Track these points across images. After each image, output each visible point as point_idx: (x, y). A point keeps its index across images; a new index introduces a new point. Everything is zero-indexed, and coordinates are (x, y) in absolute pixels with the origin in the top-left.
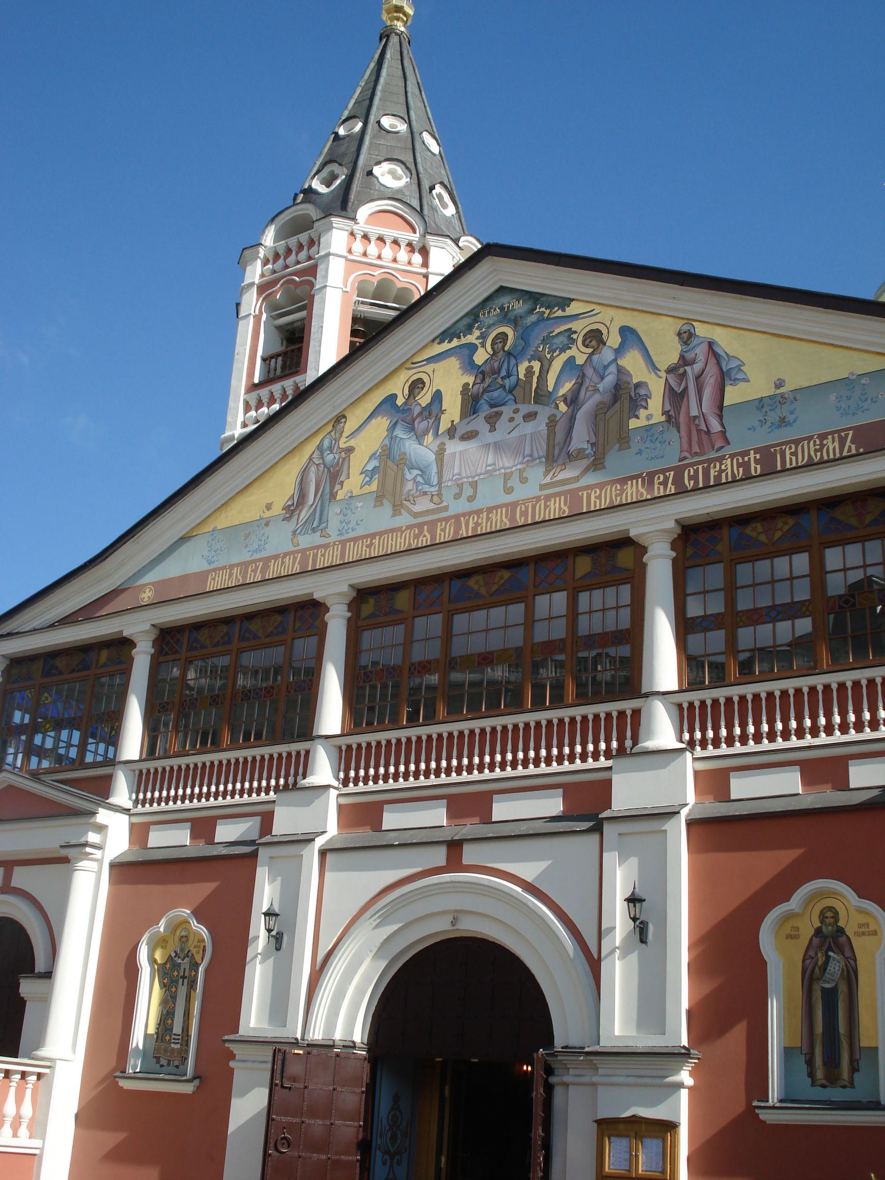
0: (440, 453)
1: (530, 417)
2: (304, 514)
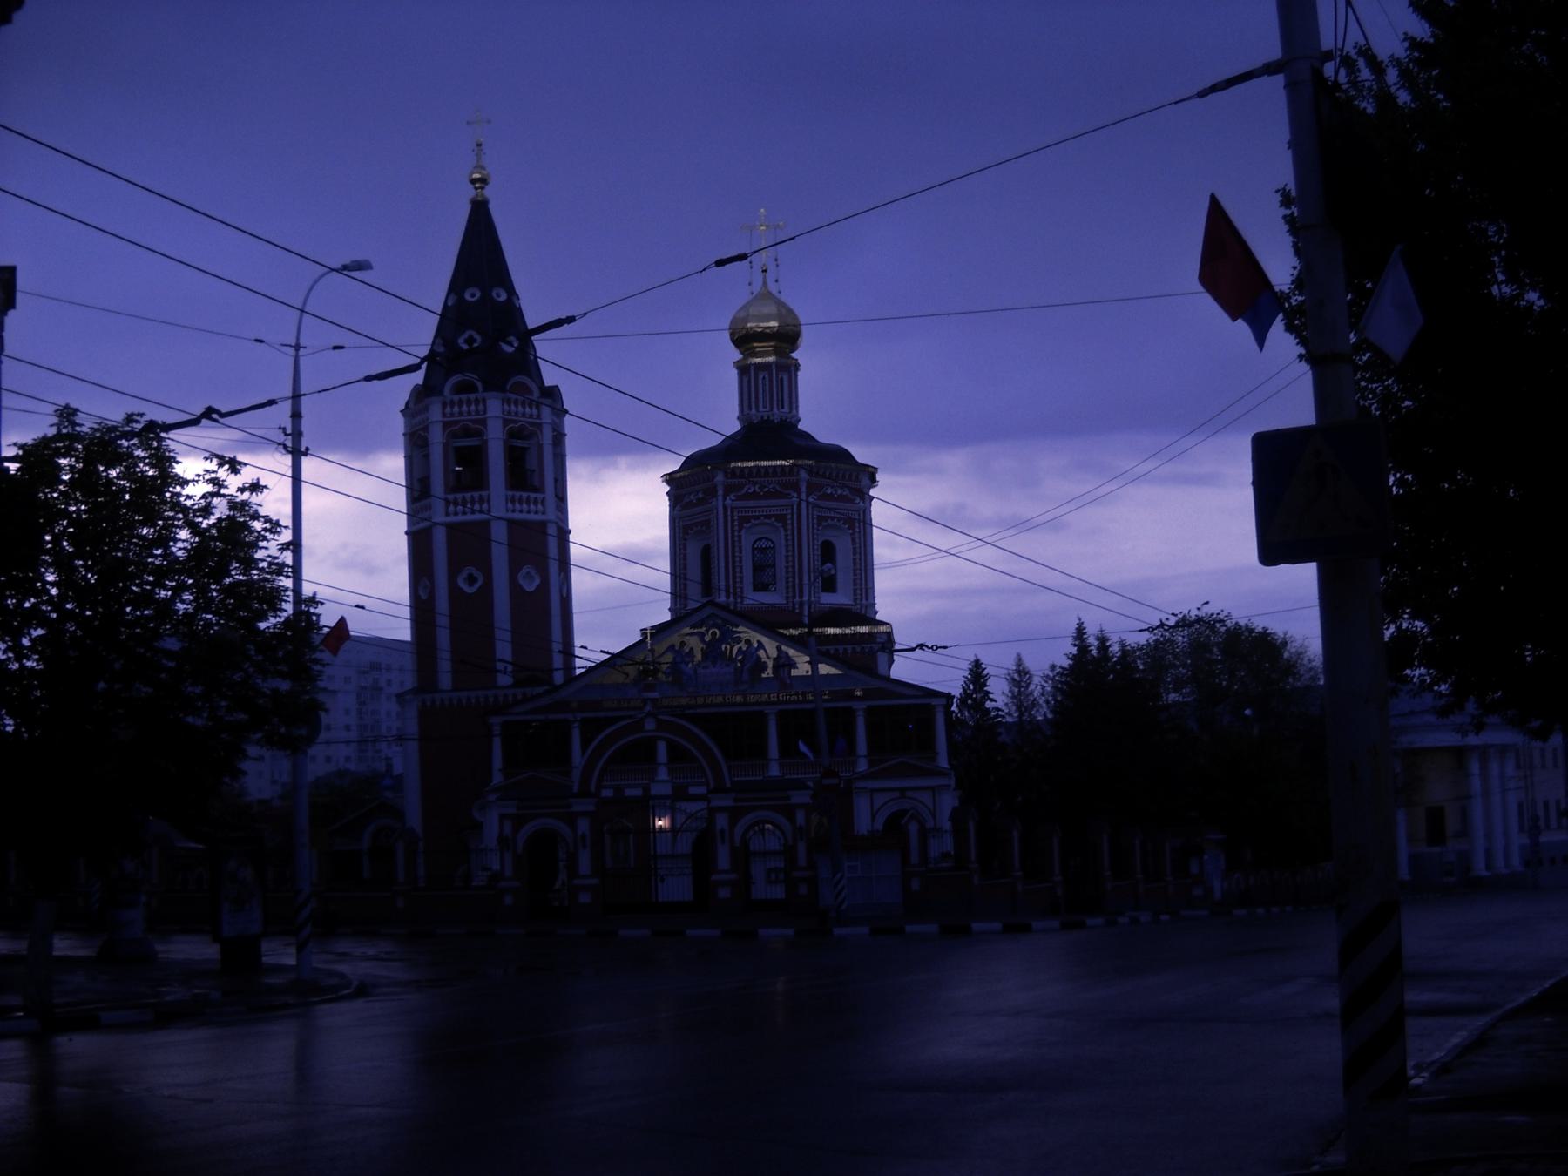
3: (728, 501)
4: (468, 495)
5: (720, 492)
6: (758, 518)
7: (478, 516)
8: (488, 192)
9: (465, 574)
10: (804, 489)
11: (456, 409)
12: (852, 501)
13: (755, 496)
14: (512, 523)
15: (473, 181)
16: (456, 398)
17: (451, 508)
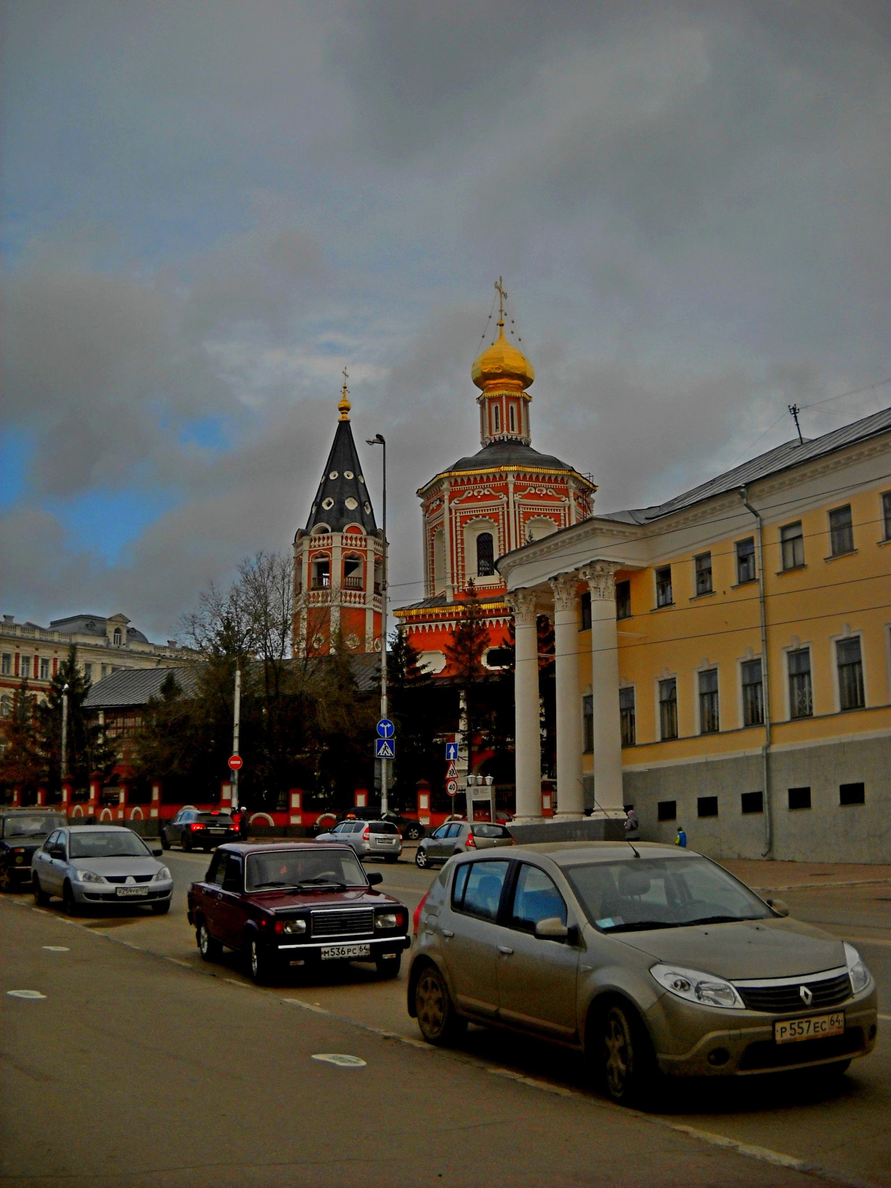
8: (349, 416)
14: (342, 608)
15: (341, 409)
16: (317, 536)
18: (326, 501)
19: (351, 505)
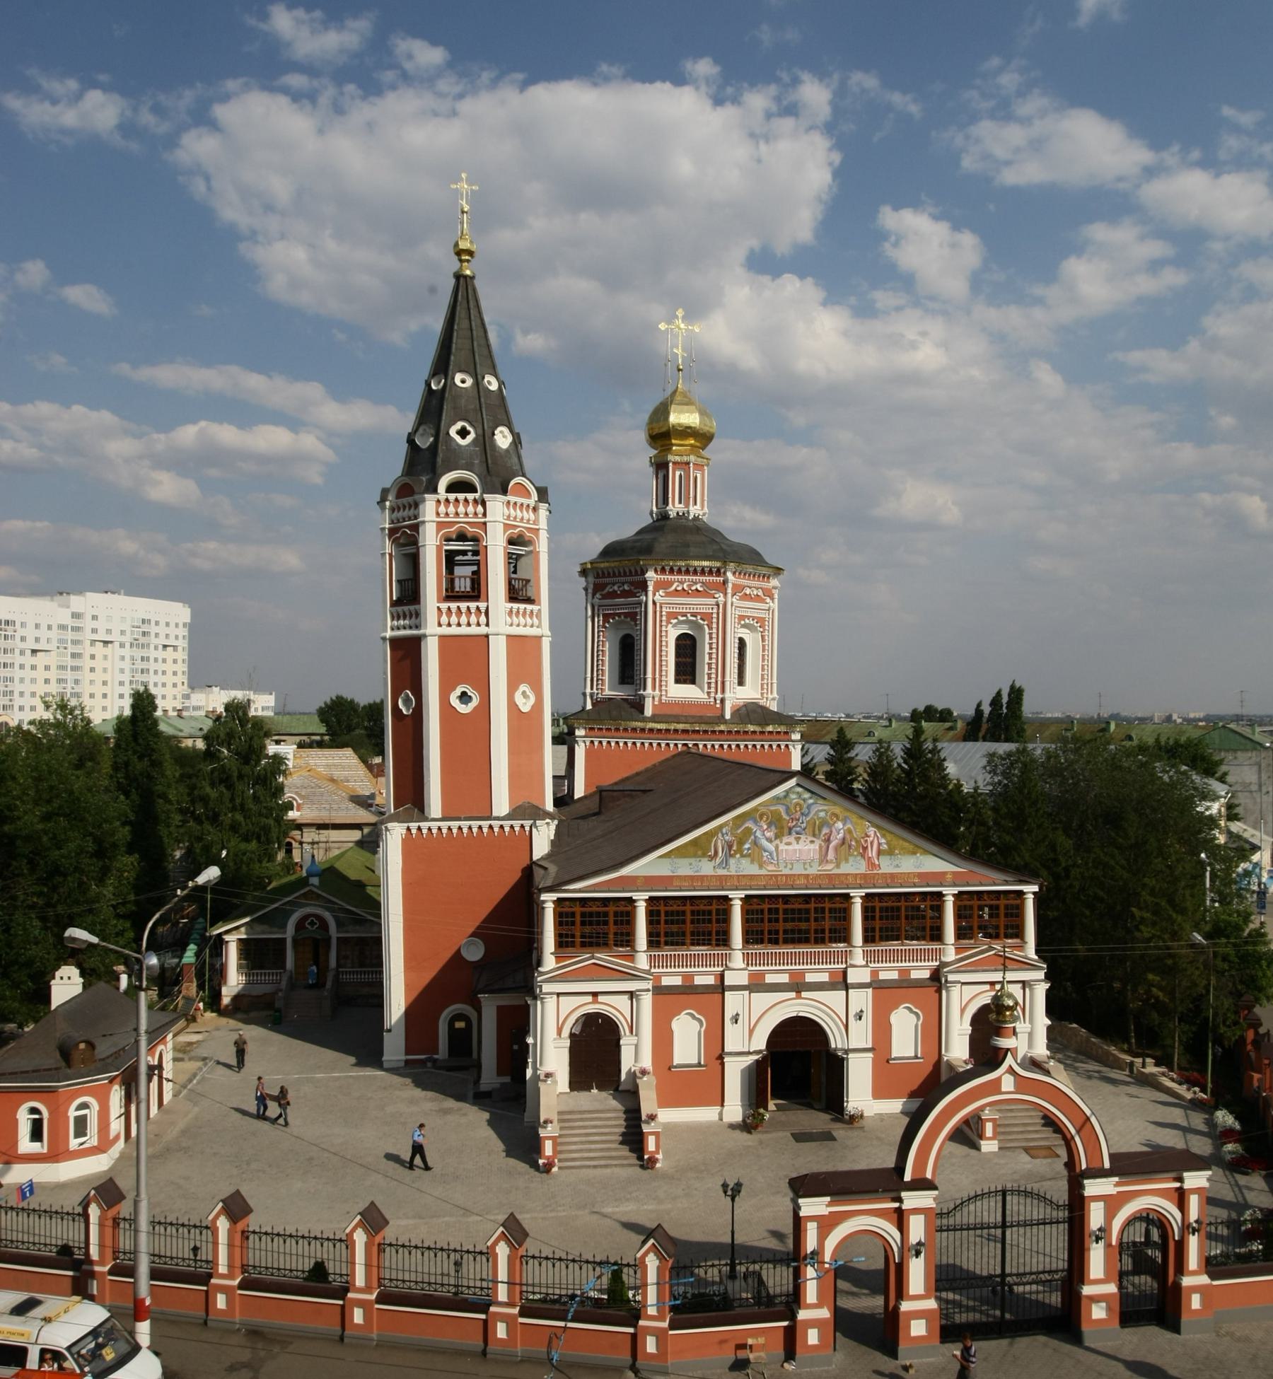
0: (777, 847)
1: (812, 842)
2: (718, 860)
3: (657, 597)
4: (463, 605)
5: (651, 588)
6: (684, 615)
7: (474, 630)
9: (458, 691)
10: (729, 591)
11: (451, 509)
12: (763, 601)
13: (684, 593)
16: (452, 496)
17: (444, 619)
18: (459, 425)
19: (503, 439)
